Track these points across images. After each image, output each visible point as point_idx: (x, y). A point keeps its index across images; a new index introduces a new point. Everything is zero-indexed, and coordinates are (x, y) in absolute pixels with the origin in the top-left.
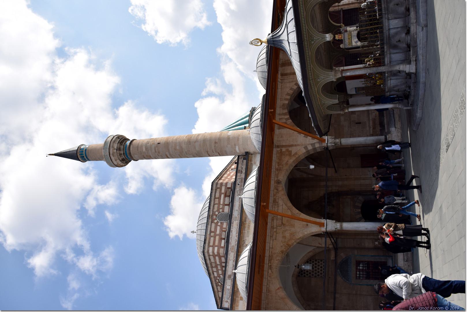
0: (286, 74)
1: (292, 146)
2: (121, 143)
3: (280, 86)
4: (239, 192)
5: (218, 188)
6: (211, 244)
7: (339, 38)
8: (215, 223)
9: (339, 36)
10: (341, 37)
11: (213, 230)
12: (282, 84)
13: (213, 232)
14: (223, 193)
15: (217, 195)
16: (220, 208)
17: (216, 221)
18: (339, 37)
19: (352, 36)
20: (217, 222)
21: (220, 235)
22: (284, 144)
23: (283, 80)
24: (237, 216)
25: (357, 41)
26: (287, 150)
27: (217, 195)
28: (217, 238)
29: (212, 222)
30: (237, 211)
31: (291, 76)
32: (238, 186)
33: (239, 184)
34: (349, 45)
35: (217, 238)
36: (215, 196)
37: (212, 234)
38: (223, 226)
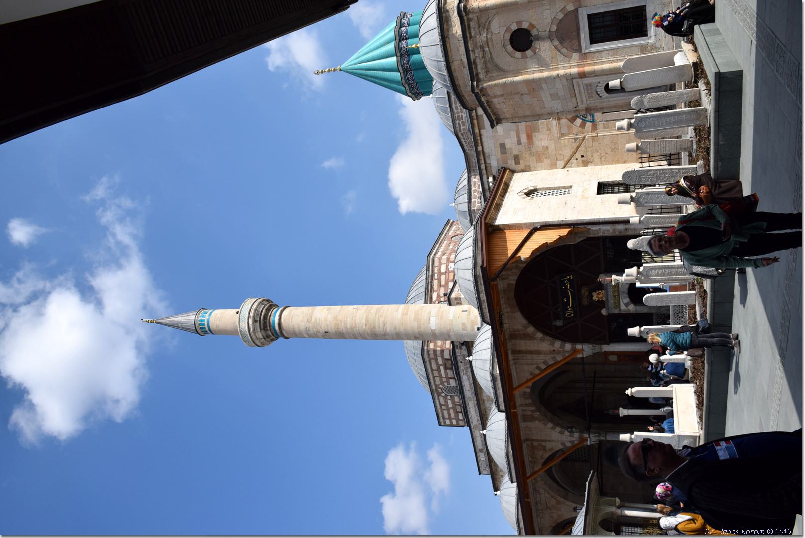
0: (520, 352)
1: (545, 441)
2: (264, 329)
3: (514, 368)
5: (433, 359)
6: (446, 416)
7: (598, 297)
8: (443, 397)
9: (598, 294)
10: (601, 295)
12: (516, 366)
15: (434, 367)
16: (444, 381)
17: (443, 394)
18: (599, 296)
21: (455, 409)
22: (534, 438)
23: (517, 359)
26: (540, 445)
27: (434, 367)
29: (439, 396)
30: (469, 391)
31: (528, 355)
32: (461, 364)
33: (462, 362)
35: (452, 411)
37: (444, 407)
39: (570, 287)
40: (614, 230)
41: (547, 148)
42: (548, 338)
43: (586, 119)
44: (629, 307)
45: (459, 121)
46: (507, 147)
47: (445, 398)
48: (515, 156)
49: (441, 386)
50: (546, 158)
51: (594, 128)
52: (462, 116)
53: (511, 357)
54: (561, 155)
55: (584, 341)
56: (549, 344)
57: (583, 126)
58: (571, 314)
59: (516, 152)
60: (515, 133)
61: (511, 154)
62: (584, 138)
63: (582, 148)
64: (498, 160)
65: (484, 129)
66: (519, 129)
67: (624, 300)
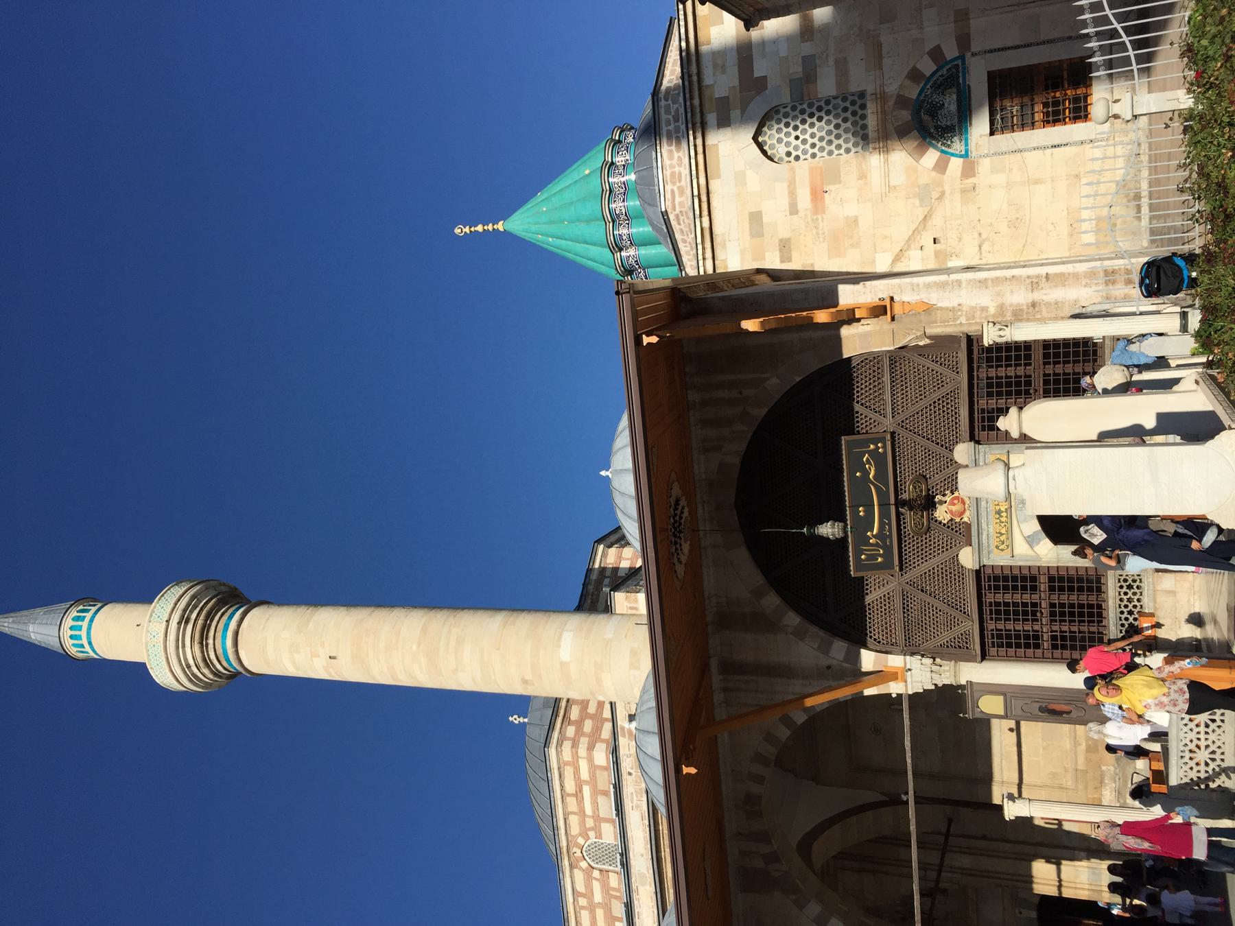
4: (635, 798)
11: (580, 888)
13: (581, 895)
14: (586, 782)
15: (570, 786)
16: (588, 826)
19: (1013, 503)
20: (587, 869)
21: (607, 908)
24: (647, 873)
25: (1036, 533)
27: (570, 786)
28: (600, 913)
30: (642, 855)
33: (630, 774)
34: (997, 547)
35: (600, 913)
36: (562, 786)
37: (582, 902)
38: (609, 884)
39: (874, 477)
40: (1001, 307)
41: (856, 220)
42: (814, 629)
43: (950, 150)
44: (1035, 549)
45: (674, 184)
46: (765, 220)
47: (589, 878)
48: (781, 241)
49: (581, 841)
50: (852, 246)
51: (969, 170)
52: (680, 174)
53: (716, 680)
54: (886, 237)
55: (911, 650)
56: (816, 646)
57: (941, 167)
58: (872, 557)
59: (784, 233)
60: (785, 185)
61: (772, 236)
62: (943, 193)
63: (937, 221)
64: (742, 252)
65: (719, 177)
66: (794, 178)
67: (1022, 526)
